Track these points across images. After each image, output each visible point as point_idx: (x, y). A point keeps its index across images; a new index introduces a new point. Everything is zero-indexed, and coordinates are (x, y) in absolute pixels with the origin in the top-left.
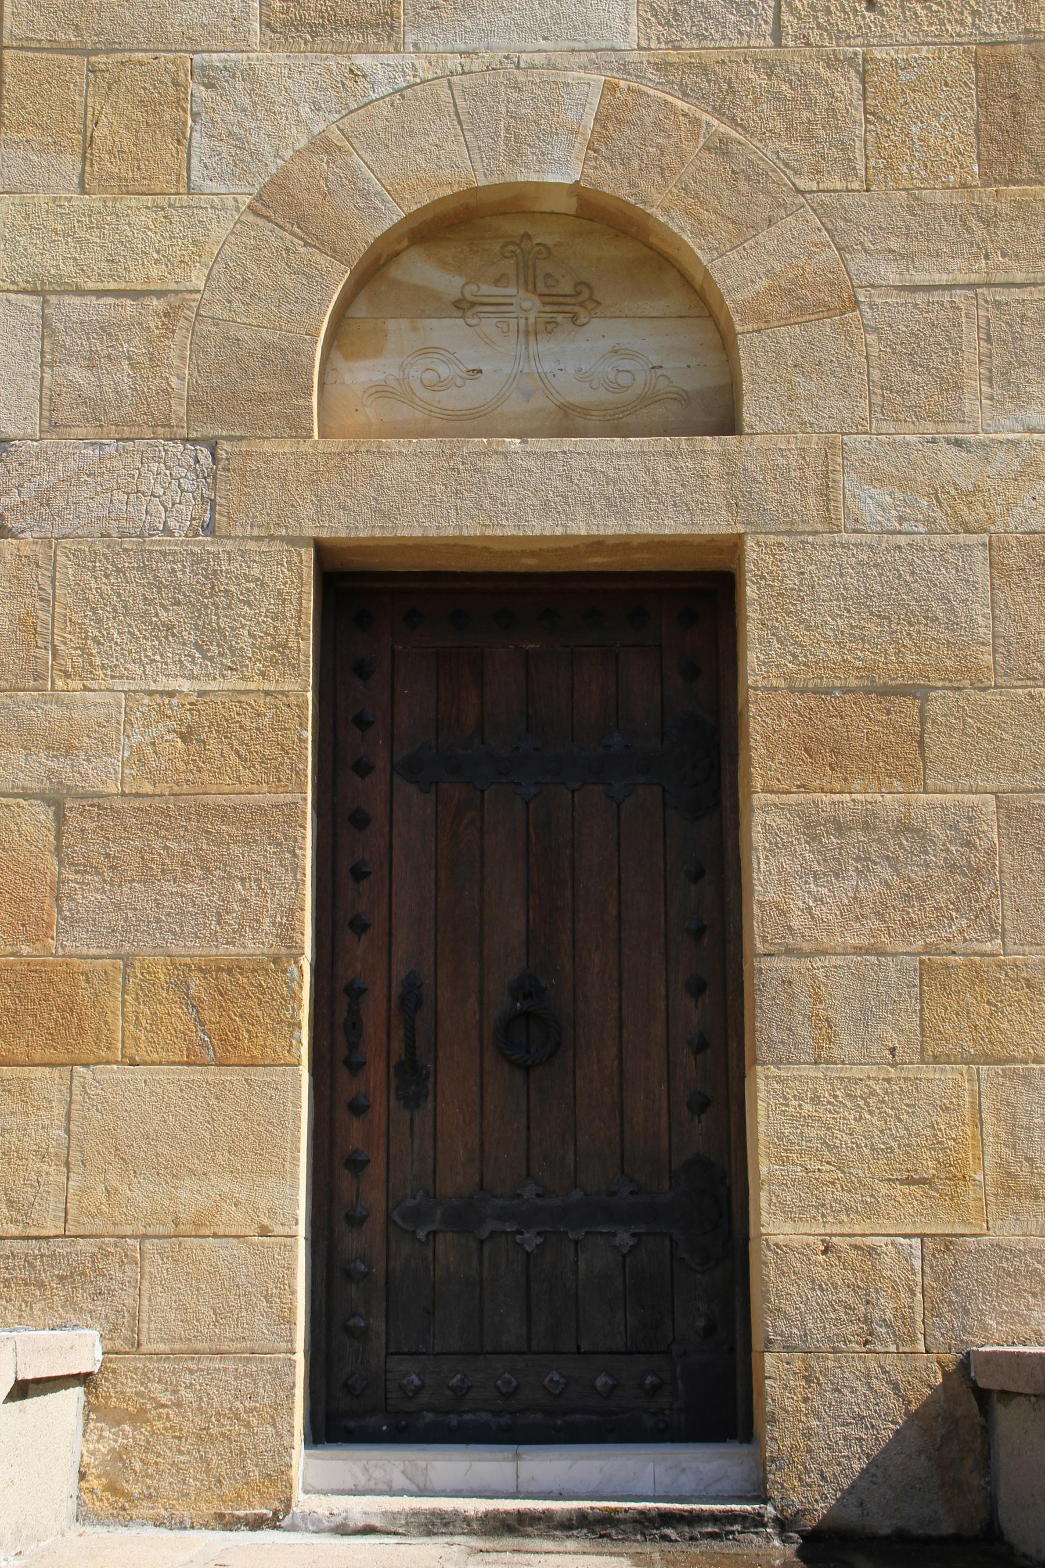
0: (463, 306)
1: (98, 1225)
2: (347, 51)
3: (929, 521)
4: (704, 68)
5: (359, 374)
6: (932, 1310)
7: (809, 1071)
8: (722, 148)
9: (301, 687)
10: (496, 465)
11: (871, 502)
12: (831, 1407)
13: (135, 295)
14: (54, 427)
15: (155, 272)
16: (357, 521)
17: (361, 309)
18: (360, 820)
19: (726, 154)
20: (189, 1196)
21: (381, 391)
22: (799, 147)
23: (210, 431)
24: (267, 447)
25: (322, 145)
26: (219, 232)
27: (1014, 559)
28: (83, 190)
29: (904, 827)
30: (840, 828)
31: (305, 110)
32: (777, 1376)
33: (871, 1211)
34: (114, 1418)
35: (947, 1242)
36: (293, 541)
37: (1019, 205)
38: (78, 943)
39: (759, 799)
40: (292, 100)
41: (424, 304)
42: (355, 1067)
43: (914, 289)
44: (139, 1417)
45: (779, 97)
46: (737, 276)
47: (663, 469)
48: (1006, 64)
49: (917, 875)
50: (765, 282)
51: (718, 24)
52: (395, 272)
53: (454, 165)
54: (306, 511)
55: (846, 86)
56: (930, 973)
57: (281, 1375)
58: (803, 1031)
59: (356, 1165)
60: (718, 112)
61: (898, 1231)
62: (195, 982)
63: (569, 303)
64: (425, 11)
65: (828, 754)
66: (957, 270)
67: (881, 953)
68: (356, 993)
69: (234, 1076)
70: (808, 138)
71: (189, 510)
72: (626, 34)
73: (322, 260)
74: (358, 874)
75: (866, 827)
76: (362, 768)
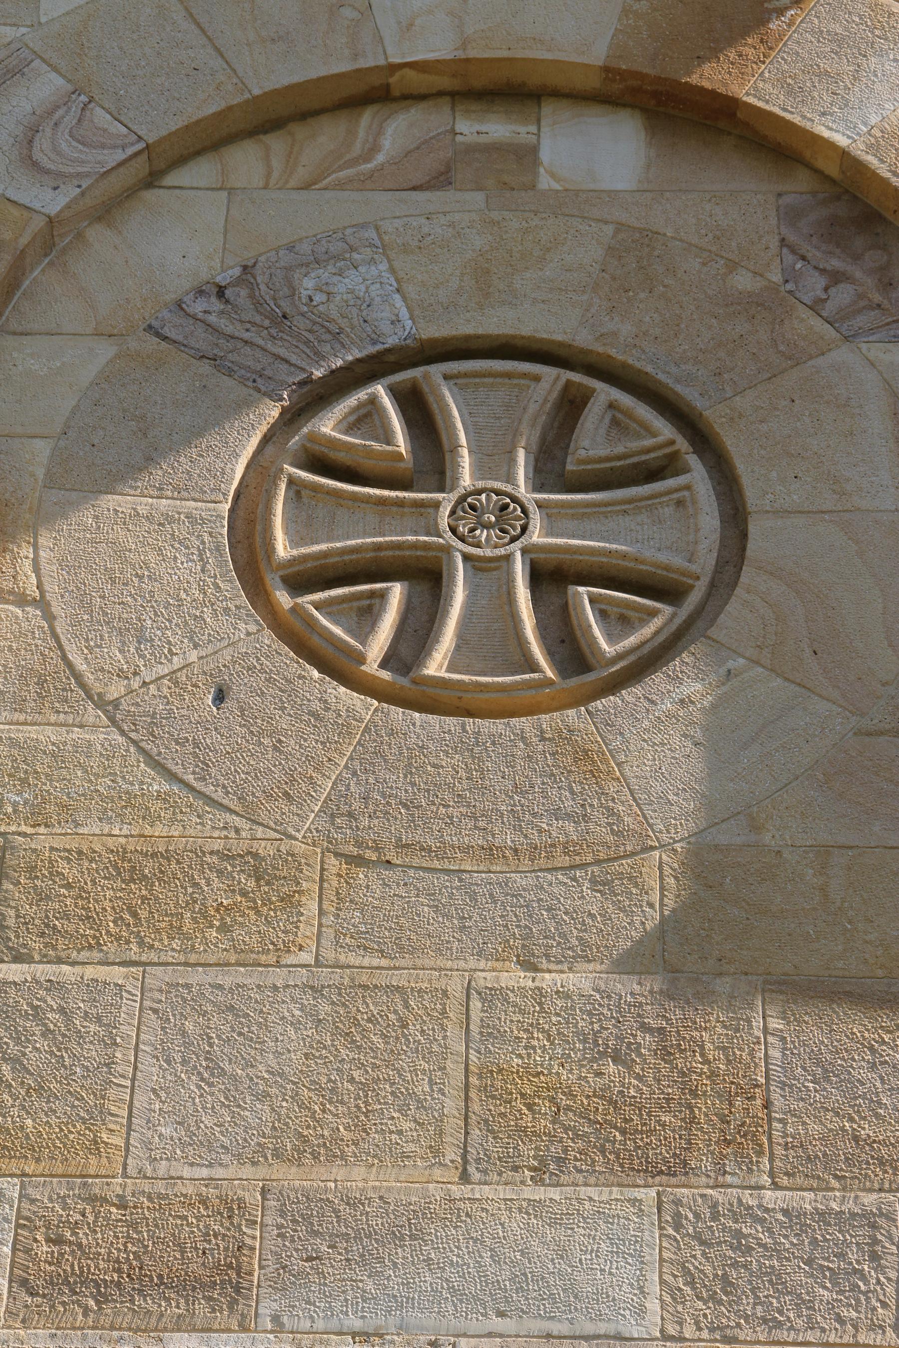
51: (800, 1303)
64: (297, 1264)
72: (641, 1311)
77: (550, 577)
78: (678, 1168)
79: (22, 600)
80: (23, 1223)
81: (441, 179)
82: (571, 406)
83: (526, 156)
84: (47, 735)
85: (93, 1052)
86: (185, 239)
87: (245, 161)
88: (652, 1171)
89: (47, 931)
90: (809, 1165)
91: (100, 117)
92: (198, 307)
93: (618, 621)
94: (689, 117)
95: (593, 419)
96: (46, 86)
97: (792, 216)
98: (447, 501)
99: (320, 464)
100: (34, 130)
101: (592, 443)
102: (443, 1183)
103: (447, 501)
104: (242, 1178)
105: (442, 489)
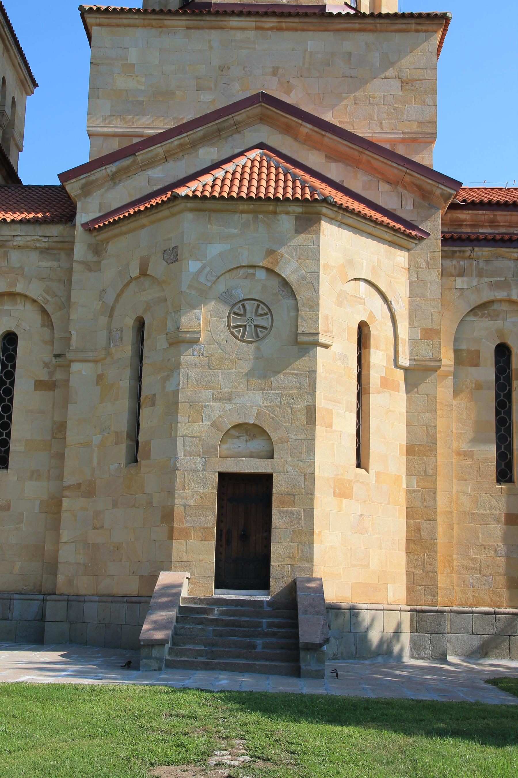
0: (238, 437)
1: (190, 560)
2: (223, 403)
3: (297, 472)
4: (271, 407)
5: (224, 446)
6: (291, 574)
7: (277, 544)
8: (273, 418)
9: (216, 491)
10: (241, 462)
11: (290, 469)
12: (277, 584)
13: (195, 437)
14: (184, 455)
15: (198, 434)
16: (224, 470)
17: (224, 437)
18: (223, 507)
19: (273, 420)
20: (201, 557)
21: (227, 449)
22: (282, 418)
23: (205, 456)
24: (212, 459)
25: (220, 416)
26: (206, 429)
27: (307, 477)
28: (188, 422)
29: (291, 513)
30: (283, 512)
31: (218, 412)
32: (272, 581)
33: (284, 561)
34: (192, 584)
35: (293, 565)
36: (215, 472)
37: (311, 428)
38: (187, 525)
39: (273, 508)
40: (216, 411)
41: (233, 437)
42: (221, 540)
43: (297, 439)
44: (195, 584)
45: (280, 411)
46: (274, 437)
47: (263, 464)
48: (310, 408)
49: (293, 519)
50: (277, 438)
52: (229, 432)
53: (237, 420)
54: (217, 467)
55: (289, 410)
56: (293, 531)
57: (212, 579)
58: (277, 539)
59: (221, 553)
60: (272, 413)
61: (287, 564)
62: (202, 530)
63: (252, 437)
65: (283, 503)
66: (302, 437)
67: (287, 529)
68: (221, 531)
69: (206, 542)
70: (284, 418)
71: (202, 467)
73: (220, 433)
74: (222, 515)
75: (286, 512)
76: (223, 500)
77: (256, 326)
78: (264, 390)
79: (209, 331)
80: (213, 394)
81: (246, 278)
82: (258, 305)
83: (254, 274)
84: (212, 346)
85: (217, 379)
86: (221, 287)
87: (227, 275)
88: (262, 390)
89: (213, 367)
90: (275, 389)
91: (213, 273)
92: (223, 295)
93: (262, 332)
94: (270, 271)
95: (260, 308)
96: (208, 269)
97: (279, 283)
98: (246, 318)
99: (235, 314)
100: (207, 275)
101: (260, 312)
102: (246, 391)
103: (246, 318)
104: (230, 391)
105: (246, 317)
